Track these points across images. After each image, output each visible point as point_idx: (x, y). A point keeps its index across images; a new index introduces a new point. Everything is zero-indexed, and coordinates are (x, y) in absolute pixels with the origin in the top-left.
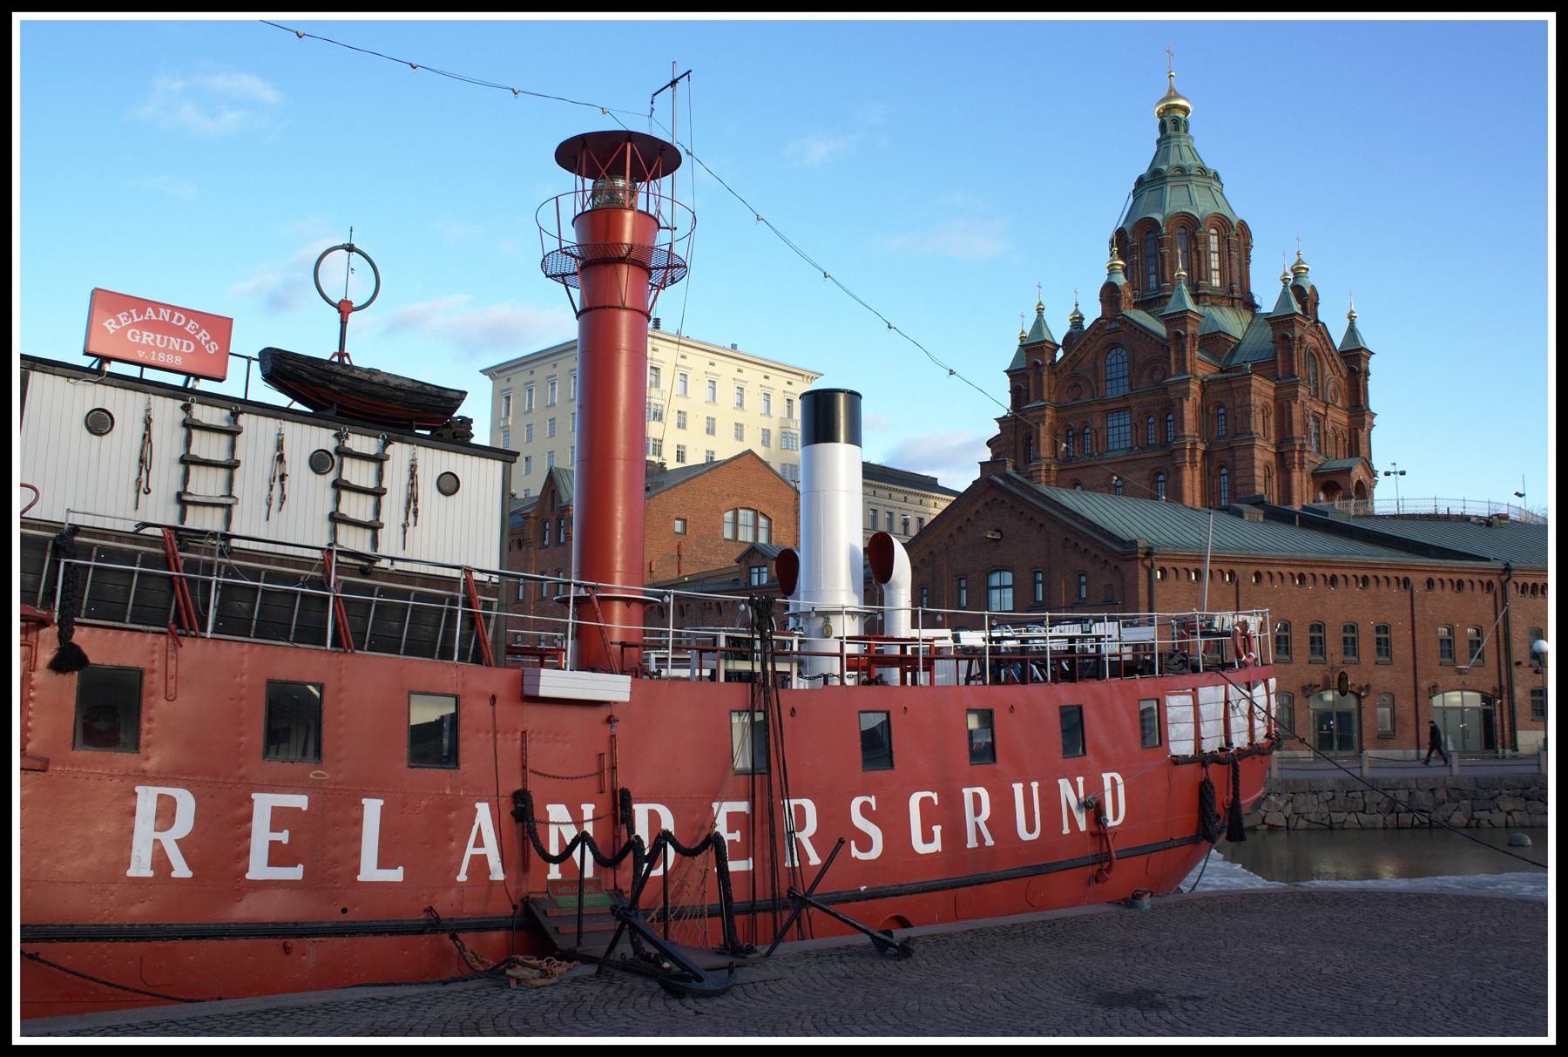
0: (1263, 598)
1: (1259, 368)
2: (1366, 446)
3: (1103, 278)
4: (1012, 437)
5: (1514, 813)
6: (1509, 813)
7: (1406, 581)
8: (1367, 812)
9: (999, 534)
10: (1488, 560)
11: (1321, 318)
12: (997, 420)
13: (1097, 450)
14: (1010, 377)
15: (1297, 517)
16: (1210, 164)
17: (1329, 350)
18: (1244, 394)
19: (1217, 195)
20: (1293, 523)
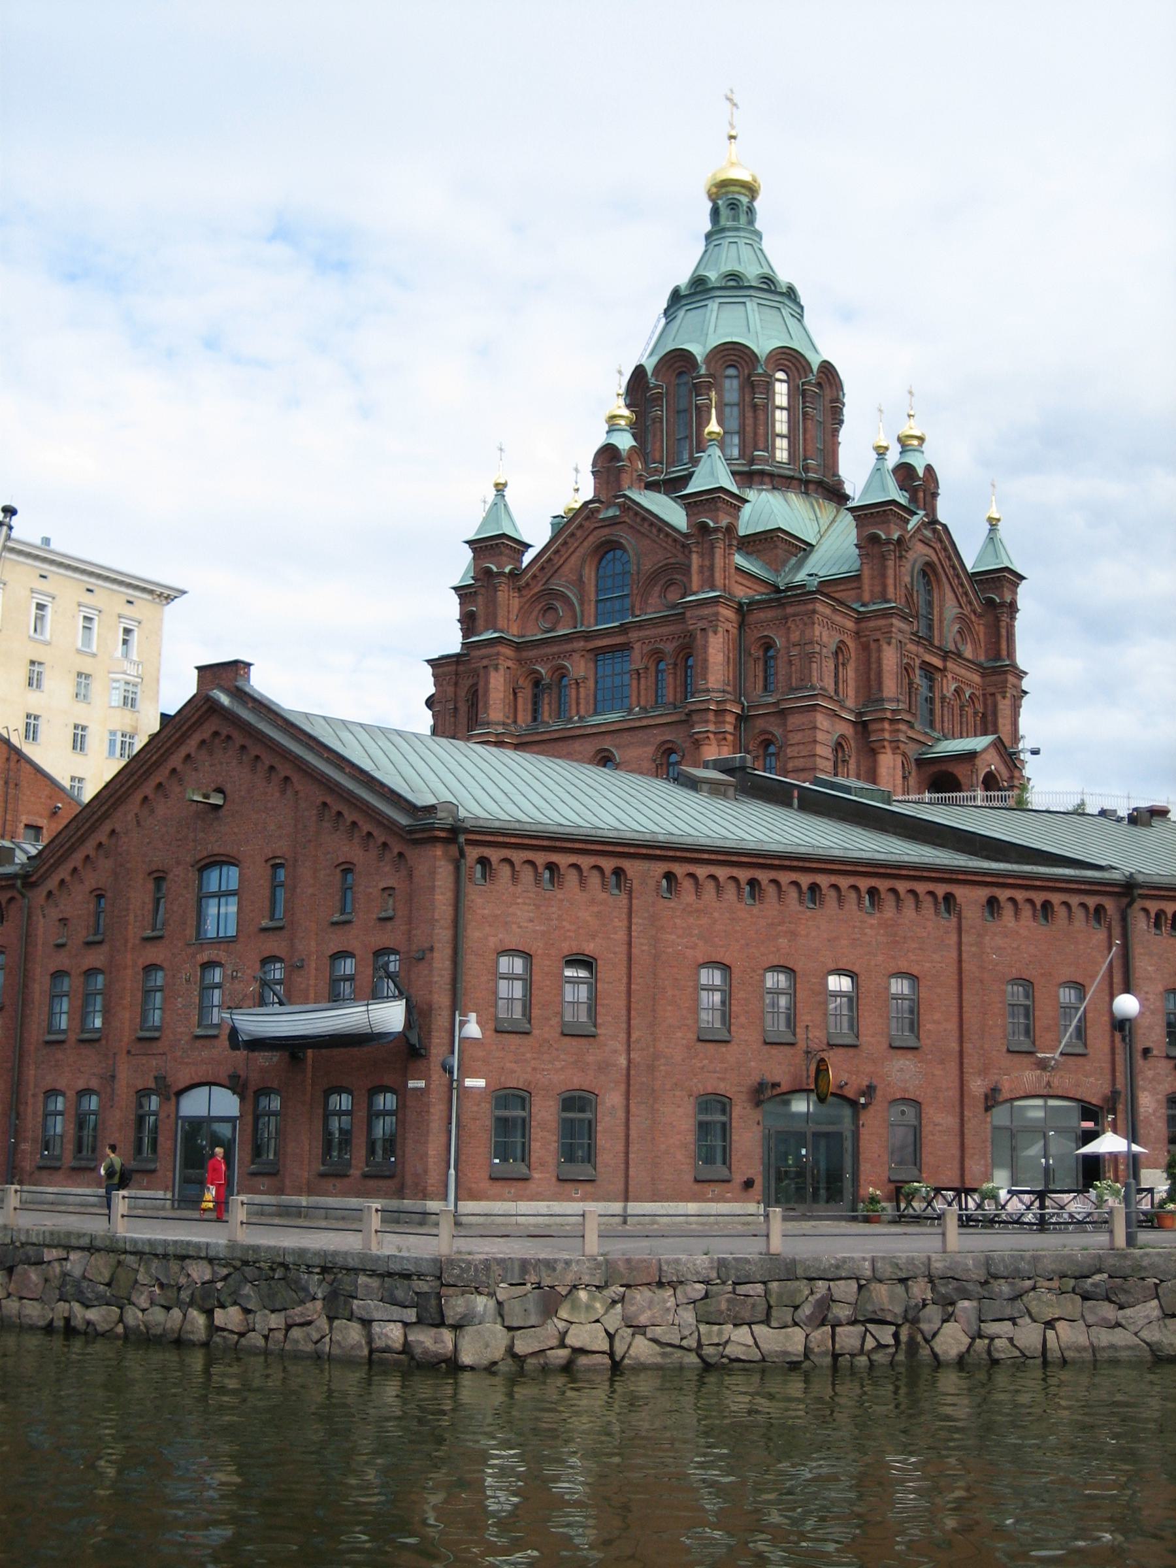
0: (678, 921)
2: (1008, 721)
3: (599, 439)
4: (450, 690)
5: (1060, 1325)
6: (1050, 1324)
7: (949, 898)
8: (774, 1324)
9: (221, 795)
11: (942, 516)
12: (428, 661)
13: (578, 712)
14: (460, 596)
15: (796, 793)
16: (784, 276)
17: (954, 568)
18: (805, 624)
19: (792, 322)
20: (787, 804)
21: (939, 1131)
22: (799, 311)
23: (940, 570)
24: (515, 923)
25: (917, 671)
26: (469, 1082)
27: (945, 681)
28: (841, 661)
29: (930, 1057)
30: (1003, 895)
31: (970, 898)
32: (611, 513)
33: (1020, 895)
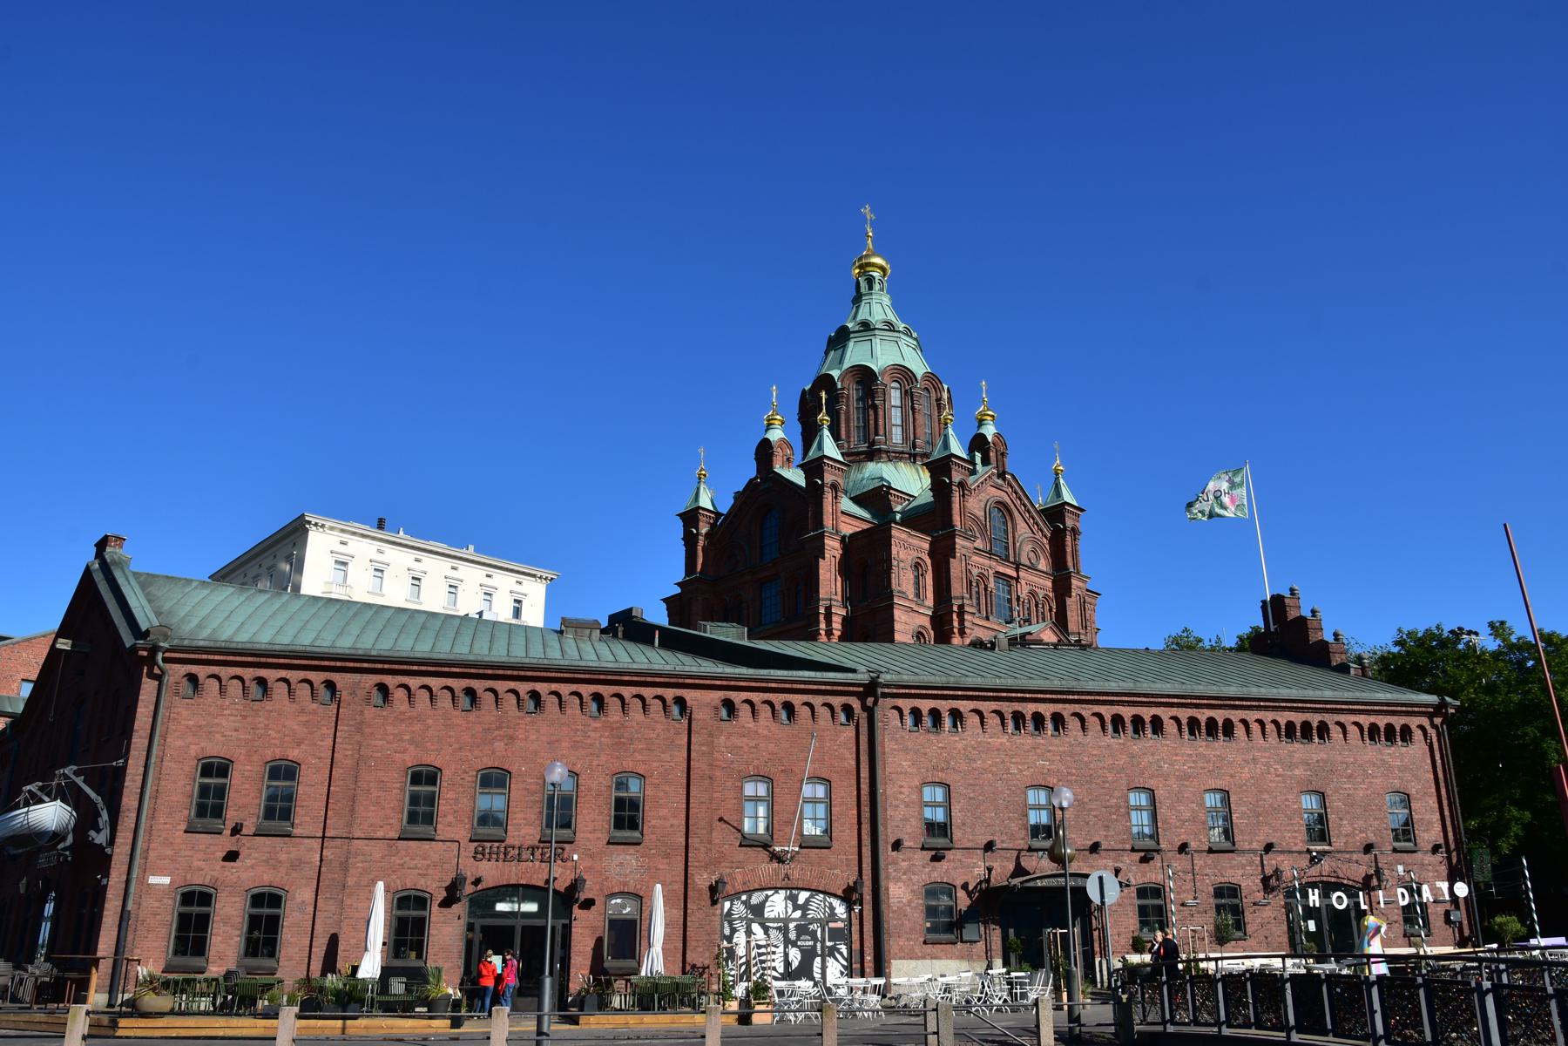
7: (680, 701)
10: (854, 671)
12: (664, 600)
17: (1025, 506)
20: (650, 643)
22: (915, 343)
23: (1012, 507)
24: (217, 732)
25: (992, 579)
26: (153, 880)
27: (1019, 586)
28: (920, 572)
31: (703, 702)
32: (766, 486)
33: (756, 697)
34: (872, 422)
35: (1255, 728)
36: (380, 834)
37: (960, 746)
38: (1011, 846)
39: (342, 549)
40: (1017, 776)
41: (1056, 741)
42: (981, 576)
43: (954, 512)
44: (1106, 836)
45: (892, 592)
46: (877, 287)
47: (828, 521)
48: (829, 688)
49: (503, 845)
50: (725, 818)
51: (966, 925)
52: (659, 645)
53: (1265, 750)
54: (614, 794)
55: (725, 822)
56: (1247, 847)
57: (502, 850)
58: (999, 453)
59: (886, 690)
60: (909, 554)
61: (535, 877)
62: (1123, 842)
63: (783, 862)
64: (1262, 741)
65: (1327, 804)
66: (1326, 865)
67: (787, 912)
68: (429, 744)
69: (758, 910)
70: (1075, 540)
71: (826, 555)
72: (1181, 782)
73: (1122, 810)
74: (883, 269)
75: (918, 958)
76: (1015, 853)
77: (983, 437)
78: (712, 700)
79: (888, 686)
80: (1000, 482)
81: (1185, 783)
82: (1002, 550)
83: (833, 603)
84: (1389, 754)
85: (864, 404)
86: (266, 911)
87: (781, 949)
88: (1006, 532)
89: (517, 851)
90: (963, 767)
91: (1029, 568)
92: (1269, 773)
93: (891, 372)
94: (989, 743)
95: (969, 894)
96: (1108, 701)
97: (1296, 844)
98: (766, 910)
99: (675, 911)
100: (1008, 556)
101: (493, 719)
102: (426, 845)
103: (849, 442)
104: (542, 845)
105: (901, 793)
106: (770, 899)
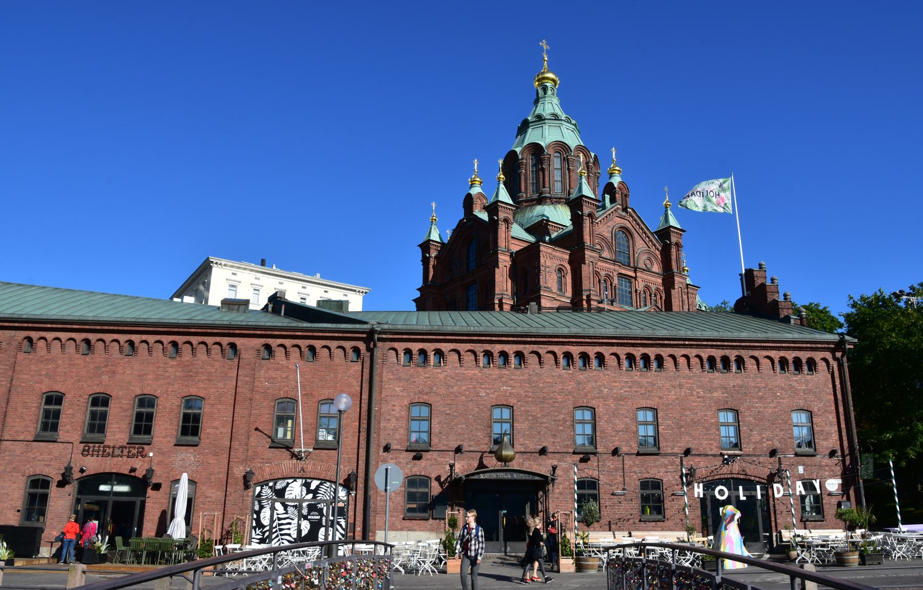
1: (557, 242)
7: (233, 346)
10: (366, 323)
17: (642, 229)
21: (210, 502)
22: (573, 127)
23: (633, 230)
29: (207, 451)
30: (274, 342)
34: (541, 180)
35: (682, 361)
36: (21, 438)
37: (441, 376)
38: (476, 449)
39: (234, 277)
40: (485, 398)
41: (518, 372)
42: (608, 276)
43: (585, 234)
44: (554, 443)
45: (540, 287)
46: (549, 92)
47: (502, 244)
48: (340, 335)
49: (102, 445)
50: (260, 428)
51: (437, 507)
52: (284, 314)
53: (690, 378)
54: (182, 411)
55: (260, 431)
56: (670, 452)
57: (102, 449)
58: (623, 195)
59: (380, 336)
60: (554, 263)
61: (123, 467)
62: (567, 447)
63: (301, 459)
64: (687, 371)
65: (740, 419)
66: (736, 467)
67: (302, 495)
68: (58, 377)
69: (280, 493)
70: (678, 251)
71: (500, 265)
72: (618, 402)
73: (567, 423)
74: (554, 81)
75: (398, 530)
76: (479, 455)
77: (612, 184)
78: (256, 345)
79: (380, 333)
80: (624, 214)
81: (621, 403)
82: (625, 258)
83: (504, 296)
84: (796, 381)
85: (536, 168)
86: (40, 491)
87: (296, 521)
88: (628, 247)
89: (111, 450)
90: (443, 391)
91: (644, 270)
92: (692, 395)
93: (554, 146)
94: (463, 374)
95: (441, 484)
96: (559, 342)
97: (711, 449)
98: (287, 493)
99: (219, 493)
100: (629, 263)
101: (102, 360)
102: (51, 445)
103: (526, 193)
104: (128, 446)
105: (393, 410)
106: (290, 485)
